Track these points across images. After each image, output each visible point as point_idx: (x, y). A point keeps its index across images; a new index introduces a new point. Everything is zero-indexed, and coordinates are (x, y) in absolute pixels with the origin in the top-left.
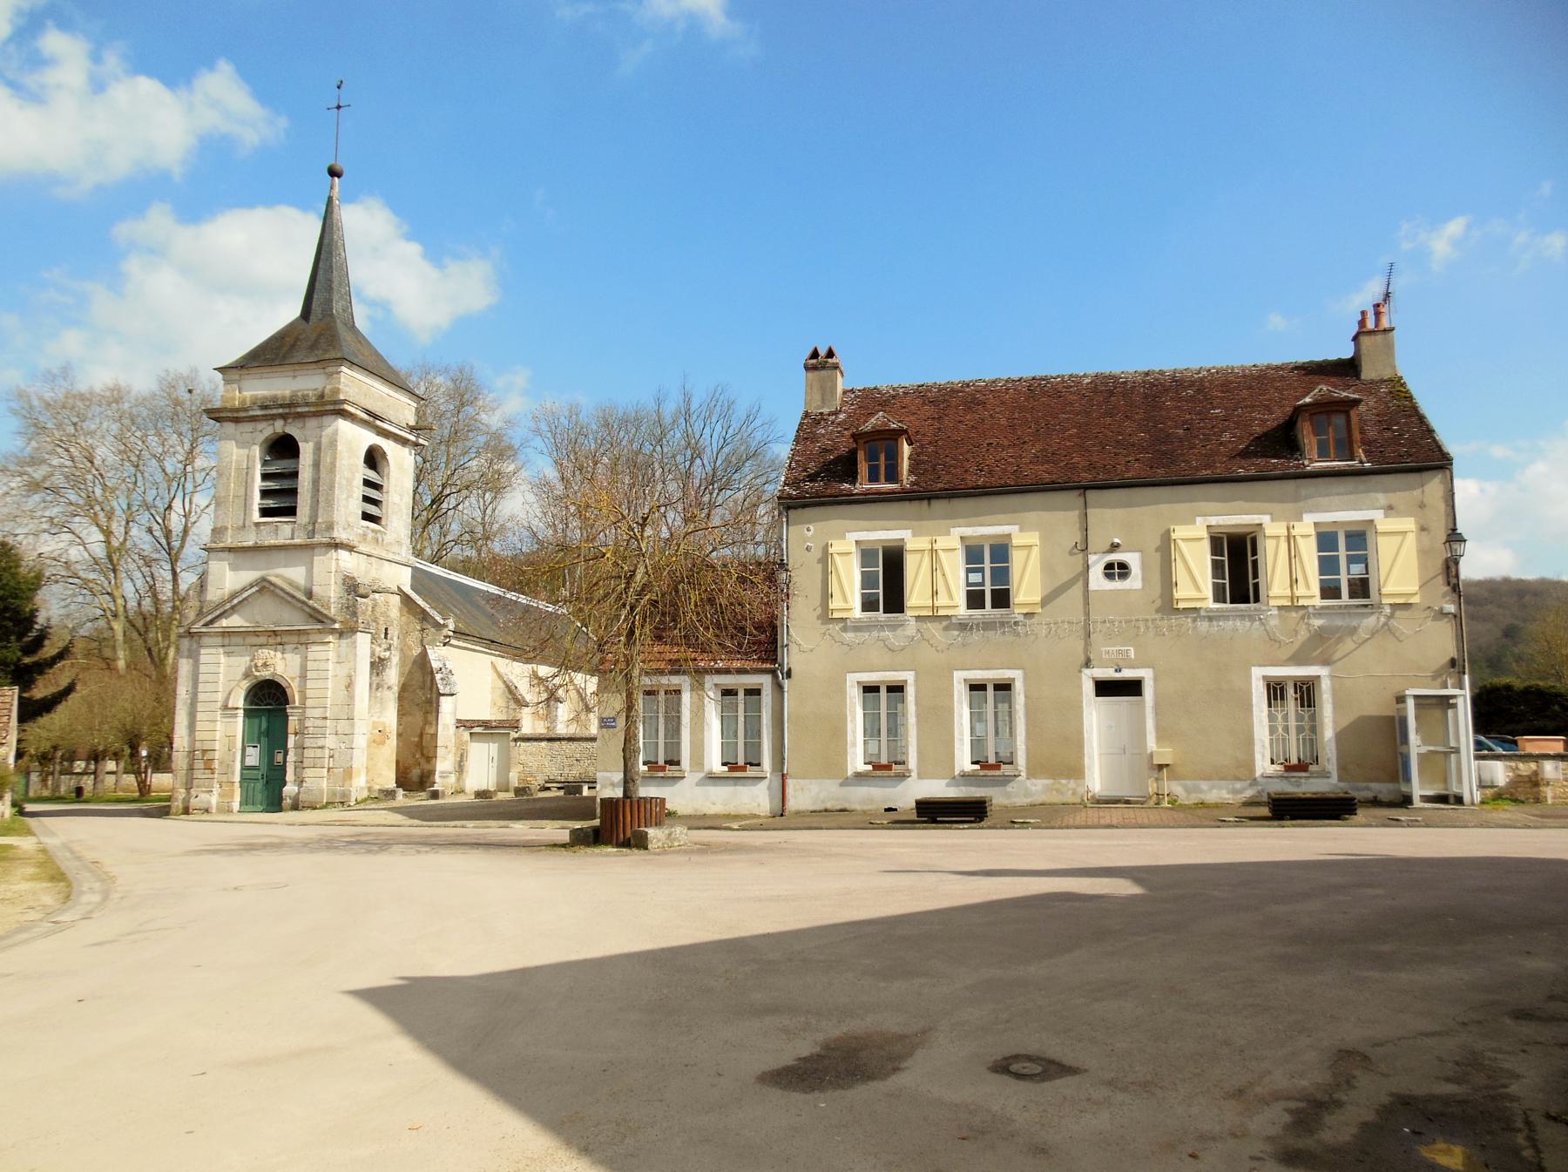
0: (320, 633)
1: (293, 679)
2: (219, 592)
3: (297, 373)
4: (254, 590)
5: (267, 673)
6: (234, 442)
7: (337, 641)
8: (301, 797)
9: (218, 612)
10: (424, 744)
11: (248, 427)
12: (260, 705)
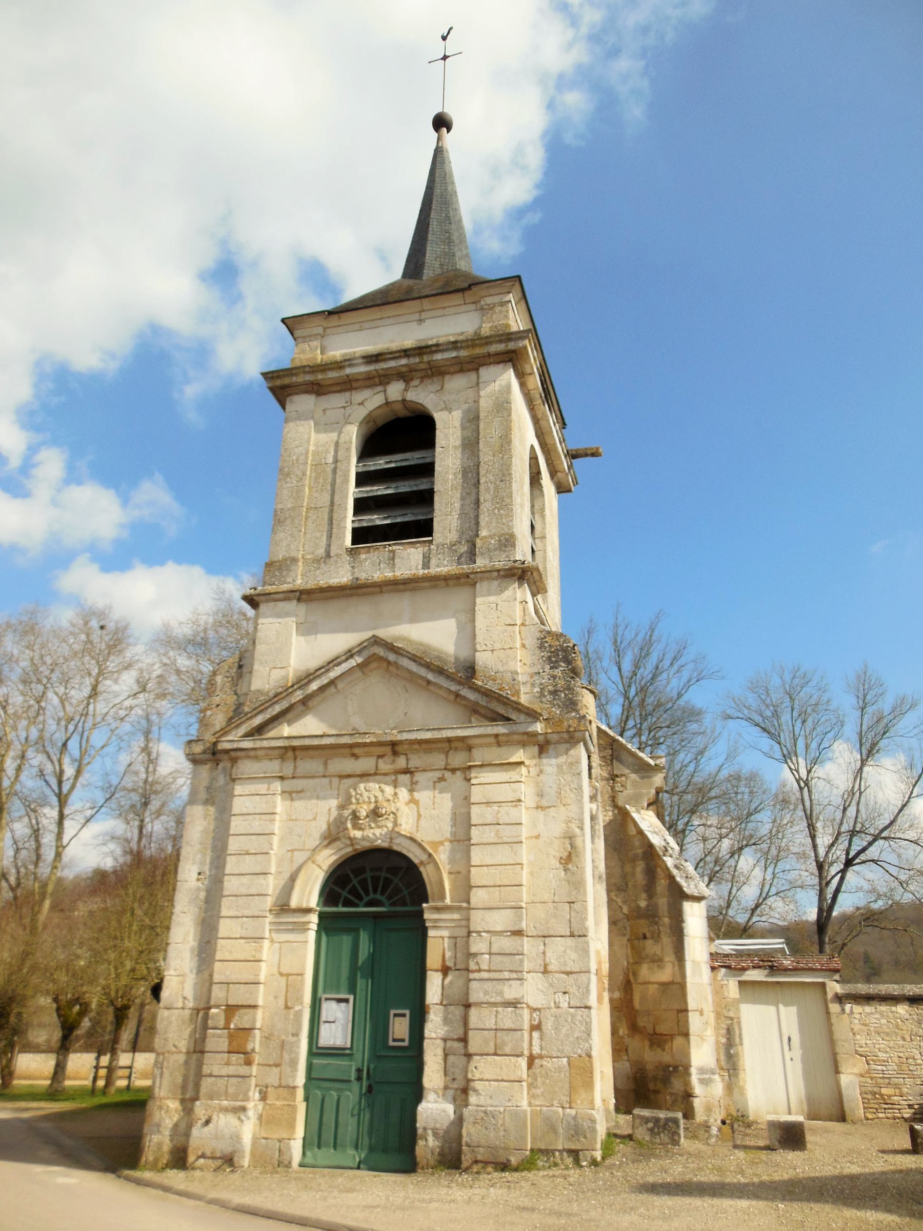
0: (499, 745)
1: (437, 844)
2: (277, 675)
3: (424, 315)
4: (352, 663)
5: (378, 832)
6: (312, 423)
7: (534, 762)
8: (470, 1132)
9: (277, 709)
10: (637, 1004)
11: (336, 400)
12: (357, 906)
